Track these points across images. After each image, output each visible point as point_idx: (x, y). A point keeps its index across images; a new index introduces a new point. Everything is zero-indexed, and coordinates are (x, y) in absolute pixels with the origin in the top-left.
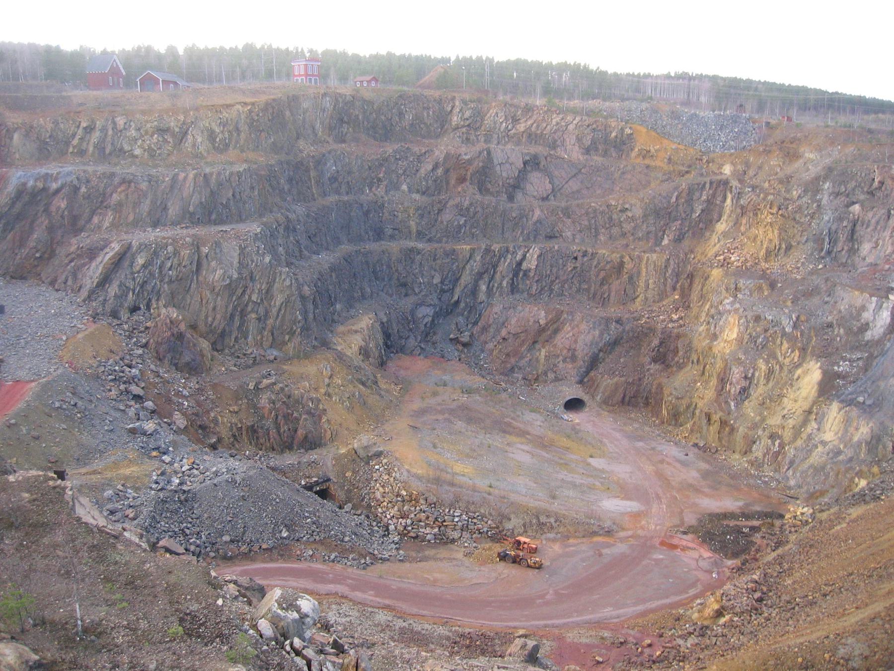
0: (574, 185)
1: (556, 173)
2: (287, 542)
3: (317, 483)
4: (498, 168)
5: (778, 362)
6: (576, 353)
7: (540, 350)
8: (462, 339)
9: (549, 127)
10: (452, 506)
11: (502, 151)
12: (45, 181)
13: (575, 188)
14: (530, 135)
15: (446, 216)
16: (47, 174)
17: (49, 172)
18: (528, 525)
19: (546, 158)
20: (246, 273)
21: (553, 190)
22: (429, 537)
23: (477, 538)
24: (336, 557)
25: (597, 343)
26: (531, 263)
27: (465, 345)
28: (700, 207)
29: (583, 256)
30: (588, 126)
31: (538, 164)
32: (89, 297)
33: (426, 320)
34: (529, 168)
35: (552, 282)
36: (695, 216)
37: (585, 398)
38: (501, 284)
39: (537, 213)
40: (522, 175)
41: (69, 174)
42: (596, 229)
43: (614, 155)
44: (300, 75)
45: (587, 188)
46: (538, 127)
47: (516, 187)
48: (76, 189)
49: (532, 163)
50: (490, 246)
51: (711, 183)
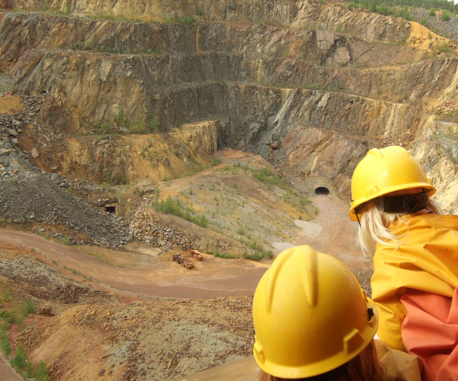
0: (365, 58)
1: (355, 49)
2: (32, 221)
3: (107, 202)
4: (318, 43)
5: (439, 176)
6: (334, 160)
7: (315, 156)
8: (273, 145)
9: (359, 21)
10: (168, 225)
14: (346, 25)
15: (280, 70)
16: (23, 15)
18: (210, 245)
19: (351, 39)
20: (111, 79)
21: (351, 59)
22: (147, 241)
23: (175, 247)
24: (58, 235)
25: (348, 156)
26: (323, 103)
27: (274, 149)
29: (357, 101)
30: (384, 21)
32: (19, 82)
33: (254, 131)
34: (338, 44)
35: (334, 116)
36: (434, 81)
37: (330, 188)
38: (303, 114)
39: (336, 72)
41: (34, 15)
42: (370, 85)
43: (396, 41)
45: (374, 60)
46: (353, 19)
47: (328, 55)
48: (35, 26)
49: (340, 41)
50: (301, 90)
51: (449, 60)
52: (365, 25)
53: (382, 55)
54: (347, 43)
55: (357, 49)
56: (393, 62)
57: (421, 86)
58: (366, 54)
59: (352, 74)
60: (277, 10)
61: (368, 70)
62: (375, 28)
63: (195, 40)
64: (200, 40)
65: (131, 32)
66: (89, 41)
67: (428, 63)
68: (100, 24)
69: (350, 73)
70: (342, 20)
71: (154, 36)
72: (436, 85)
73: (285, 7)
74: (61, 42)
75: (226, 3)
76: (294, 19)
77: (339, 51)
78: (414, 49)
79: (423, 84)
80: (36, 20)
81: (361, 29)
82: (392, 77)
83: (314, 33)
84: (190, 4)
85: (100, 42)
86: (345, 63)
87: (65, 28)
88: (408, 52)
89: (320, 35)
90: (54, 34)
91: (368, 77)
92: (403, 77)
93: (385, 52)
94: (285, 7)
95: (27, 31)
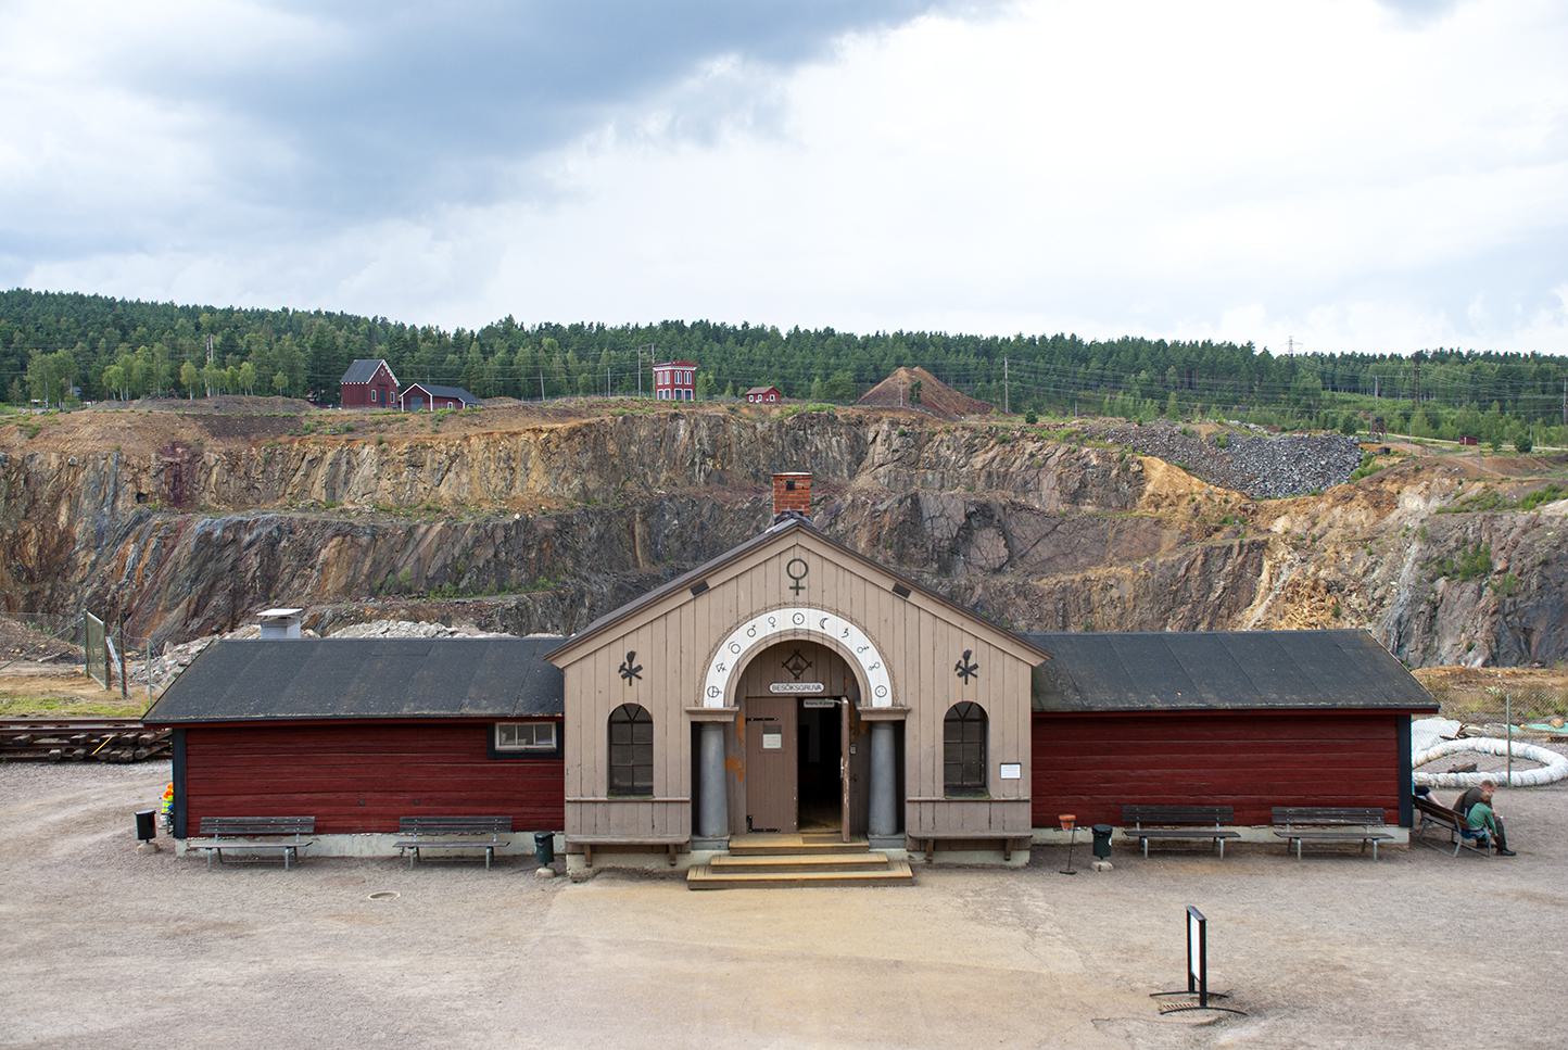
0: (1044, 550)
1: (1018, 531)
4: (928, 524)
11: (937, 498)
12: (237, 531)
13: (1045, 555)
14: (990, 475)
16: (241, 521)
17: (244, 519)
19: (1004, 509)
21: (1010, 557)
28: (1222, 583)
30: (1078, 460)
31: (992, 516)
34: (975, 524)
36: (1213, 596)
39: (979, 590)
40: (966, 533)
44: (664, 387)
47: (954, 551)
48: (273, 543)
49: (982, 515)
52: (1033, 472)
53: (1083, 540)
54: (997, 517)
55: (1024, 529)
56: (1111, 555)
57: (1185, 609)
58: (1046, 541)
59: (1018, 595)
60: (817, 448)
61: (1054, 582)
62: (1059, 478)
63: (634, 541)
64: (644, 541)
65: (498, 542)
66: (406, 571)
67: (1192, 556)
68: (427, 531)
69: (1012, 592)
70: (978, 461)
71: (545, 545)
72: (1220, 606)
73: (834, 440)
74: (343, 581)
75: (693, 443)
76: (861, 466)
77: (980, 540)
78: (1158, 522)
79: (1190, 606)
80: (275, 534)
81: (1026, 483)
82: (1115, 593)
83: (915, 500)
84: (611, 455)
85: (431, 573)
86: (997, 566)
87: (350, 547)
88: (1146, 531)
89: (930, 506)
90: (326, 563)
91: (1059, 596)
92: (1141, 591)
93: (1091, 532)
94: (834, 440)
95: (254, 562)
